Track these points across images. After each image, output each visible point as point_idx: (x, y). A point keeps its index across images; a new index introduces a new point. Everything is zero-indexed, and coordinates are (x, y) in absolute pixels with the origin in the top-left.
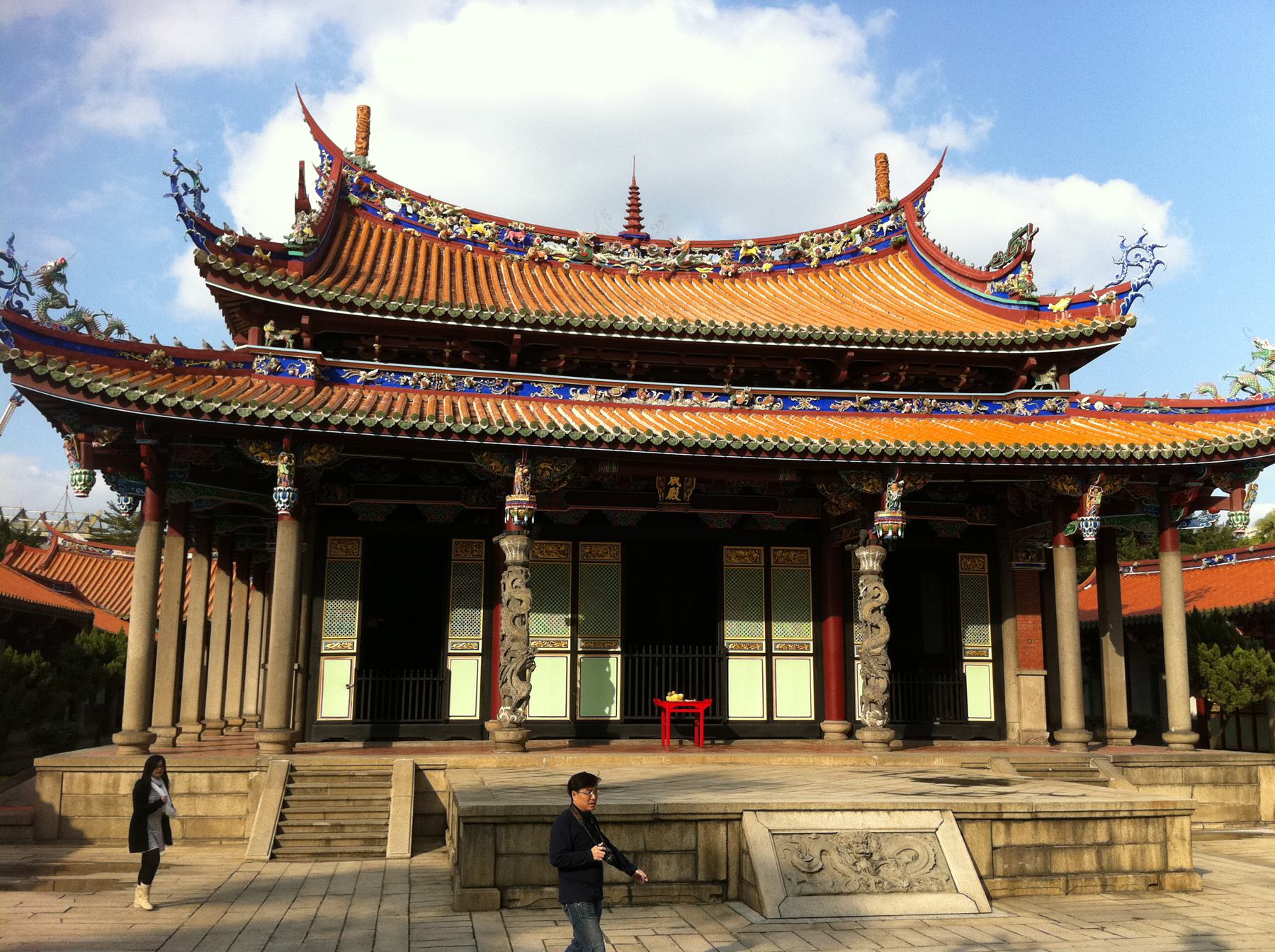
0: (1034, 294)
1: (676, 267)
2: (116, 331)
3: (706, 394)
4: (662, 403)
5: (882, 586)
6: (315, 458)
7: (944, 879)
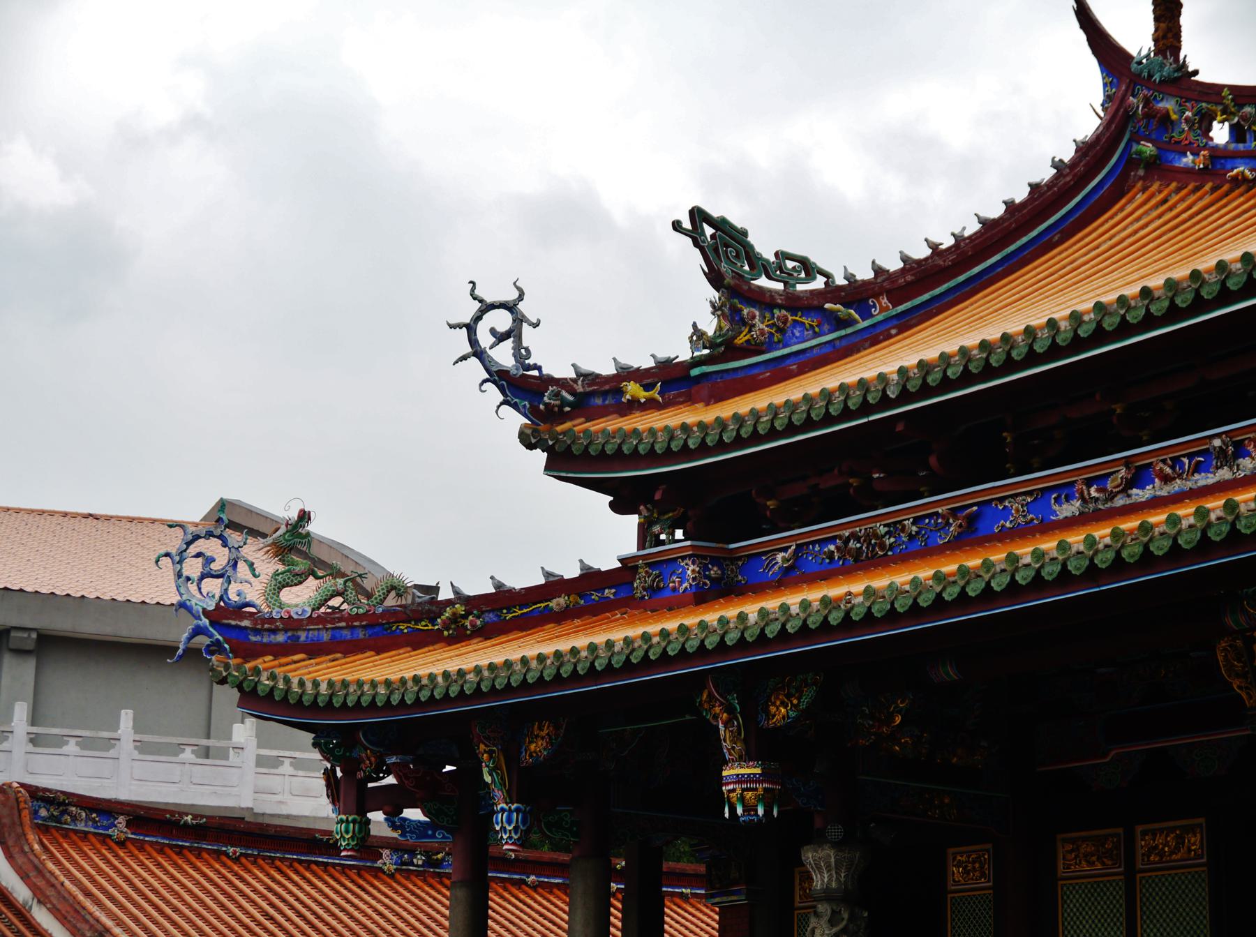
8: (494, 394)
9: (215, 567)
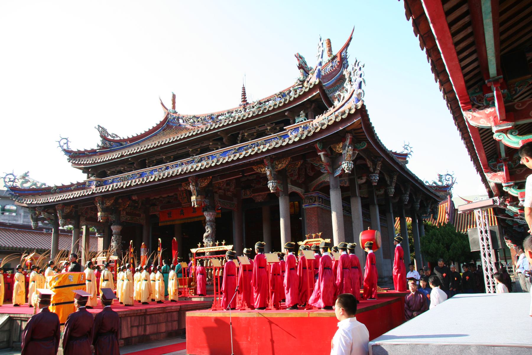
8: (63, 153)
9: (12, 180)
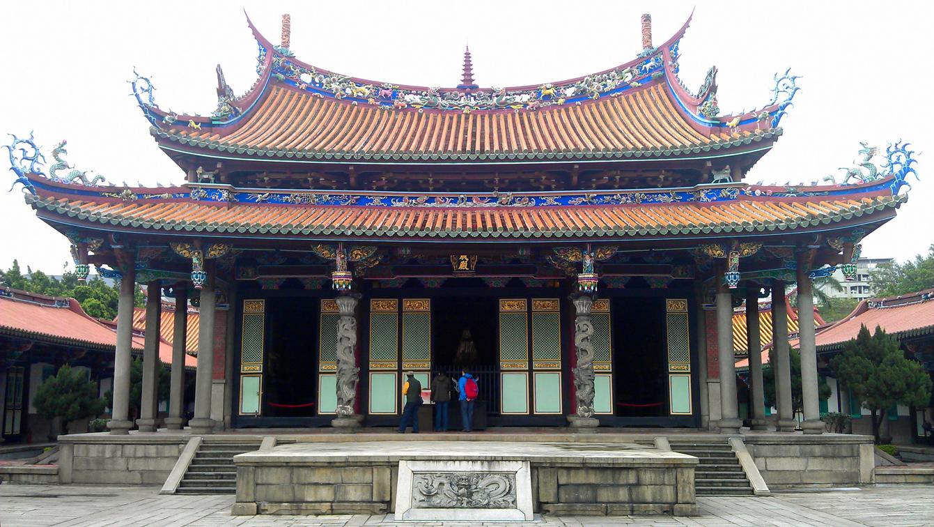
0: (718, 116)
1: (496, 106)
2: (100, 180)
3: (482, 199)
4: (453, 205)
5: (588, 323)
6: (215, 252)
7: (510, 501)
9: (28, 155)
